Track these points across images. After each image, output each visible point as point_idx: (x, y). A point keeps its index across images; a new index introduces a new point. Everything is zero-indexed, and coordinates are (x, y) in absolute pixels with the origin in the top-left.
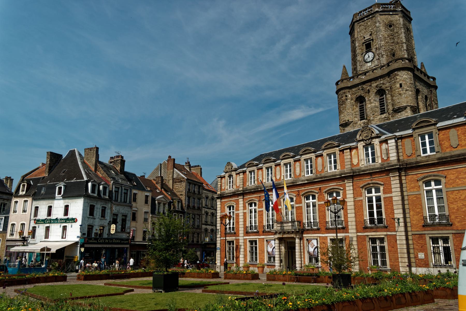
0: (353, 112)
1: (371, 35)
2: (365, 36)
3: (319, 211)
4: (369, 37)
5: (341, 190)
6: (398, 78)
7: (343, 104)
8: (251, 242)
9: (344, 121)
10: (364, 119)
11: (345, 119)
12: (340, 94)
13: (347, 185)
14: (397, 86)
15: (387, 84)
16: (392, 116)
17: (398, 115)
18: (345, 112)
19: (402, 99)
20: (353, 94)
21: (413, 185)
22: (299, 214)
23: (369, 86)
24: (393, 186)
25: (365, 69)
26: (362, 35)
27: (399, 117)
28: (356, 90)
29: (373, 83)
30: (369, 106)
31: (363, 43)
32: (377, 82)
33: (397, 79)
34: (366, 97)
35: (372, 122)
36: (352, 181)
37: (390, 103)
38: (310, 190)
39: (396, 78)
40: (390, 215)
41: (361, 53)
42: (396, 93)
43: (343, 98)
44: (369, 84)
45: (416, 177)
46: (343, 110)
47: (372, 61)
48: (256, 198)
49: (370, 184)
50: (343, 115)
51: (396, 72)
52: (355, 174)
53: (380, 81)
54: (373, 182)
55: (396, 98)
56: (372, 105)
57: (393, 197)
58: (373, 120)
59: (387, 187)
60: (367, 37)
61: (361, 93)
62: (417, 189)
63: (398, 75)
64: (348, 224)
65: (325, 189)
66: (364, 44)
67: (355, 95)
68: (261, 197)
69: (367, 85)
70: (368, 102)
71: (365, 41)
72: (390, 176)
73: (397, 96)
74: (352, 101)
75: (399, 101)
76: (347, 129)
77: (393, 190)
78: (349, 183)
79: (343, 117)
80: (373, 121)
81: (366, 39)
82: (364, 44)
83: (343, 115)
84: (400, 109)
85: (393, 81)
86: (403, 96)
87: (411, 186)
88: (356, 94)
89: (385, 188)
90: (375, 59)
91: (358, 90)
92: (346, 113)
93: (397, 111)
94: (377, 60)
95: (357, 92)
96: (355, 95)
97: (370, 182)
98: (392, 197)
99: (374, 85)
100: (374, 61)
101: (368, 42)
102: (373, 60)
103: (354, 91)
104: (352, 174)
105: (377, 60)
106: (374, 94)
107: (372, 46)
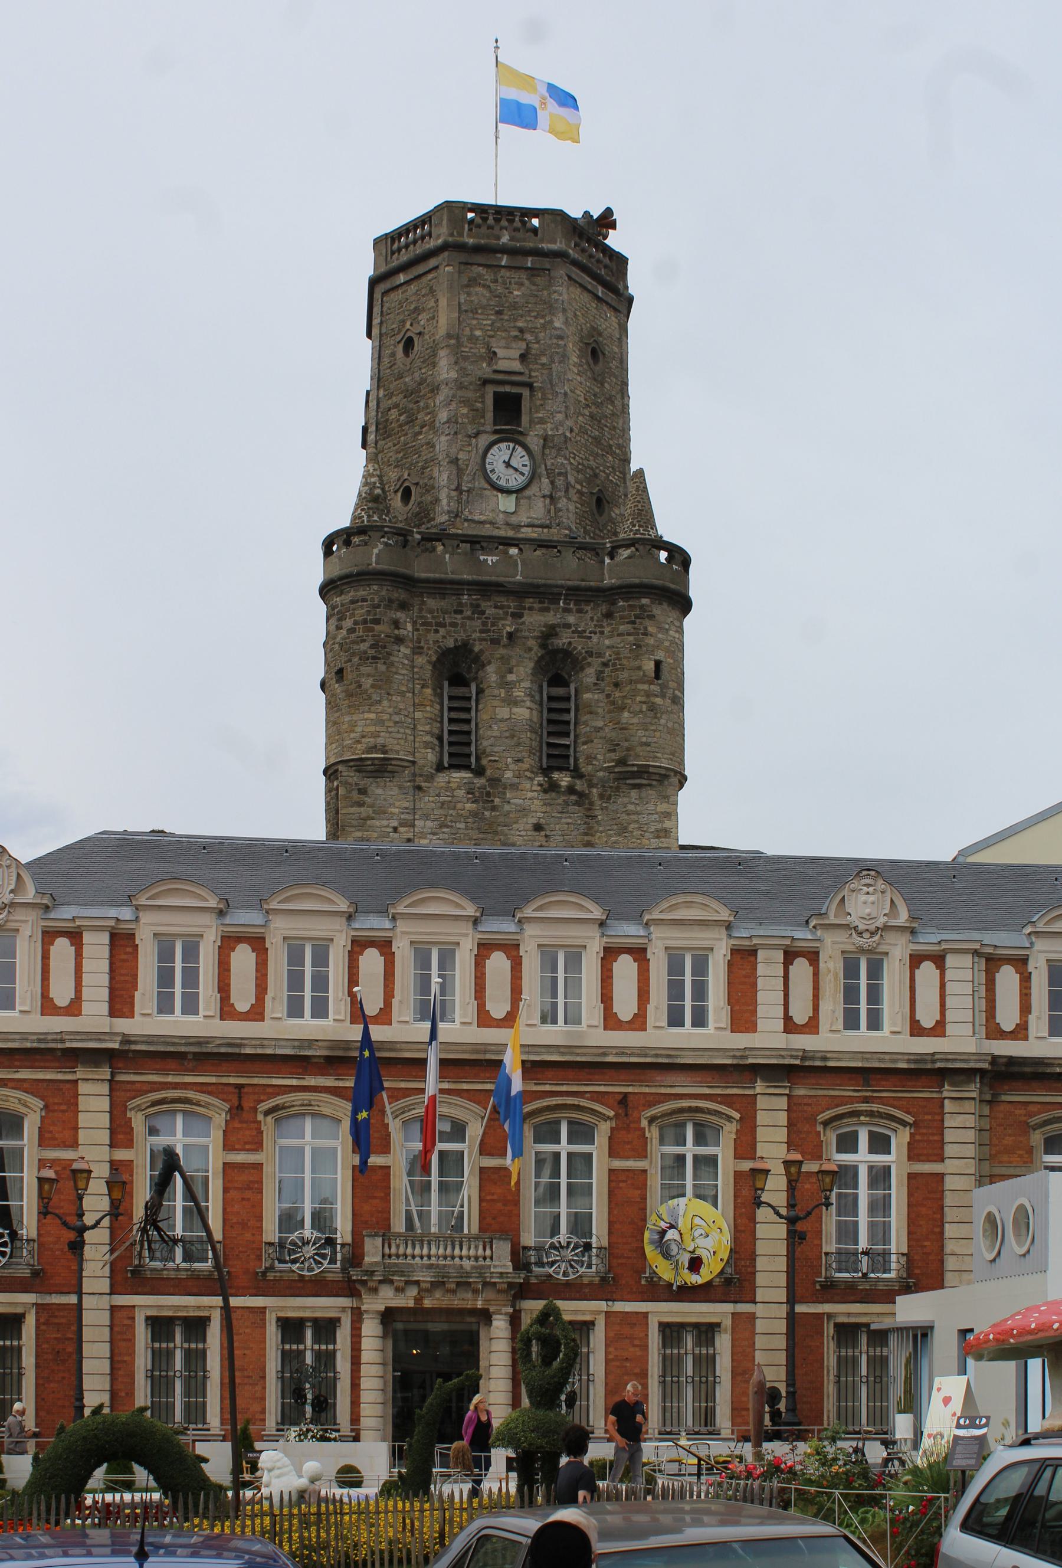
0: (418, 715)
1: (523, 357)
2: (501, 353)
3: (610, 1202)
4: (517, 366)
5: (729, 1118)
6: (650, 629)
7: (374, 658)
8: (291, 1328)
9: (373, 749)
10: (467, 767)
11: (380, 741)
12: (364, 600)
13: (761, 1103)
14: (645, 668)
15: (595, 638)
16: (601, 796)
17: (626, 800)
18: (385, 703)
19: (658, 734)
20: (423, 624)
21: (1008, 1141)
22: (499, 1205)
23: (513, 615)
24: (949, 1136)
25: (483, 518)
26: (478, 333)
27: (631, 807)
28: (445, 612)
29: (531, 609)
30: (503, 712)
31: (486, 382)
32: (547, 610)
33: (645, 634)
34: (489, 663)
35: (508, 795)
36: (787, 1091)
37: (598, 729)
38: (570, 1101)
39: (646, 628)
40: (926, 1243)
41: (471, 430)
42: (639, 699)
43: (377, 627)
44: (512, 604)
45: (1023, 1112)
46: (373, 686)
47: (518, 491)
48: (209, 1093)
49: (859, 1116)
50: (372, 716)
51: (645, 601)
52: (807, 1064)
53: (566, 610)
54: (875, 1107)
55: (635, 720)
56: (515, 710)
57: (947, 1179)
58: (514, 787)
59: (923, 1134)
60: (508, 359)
61: (472, 631)
62: (1021, 1156)
63: (652, 617)
64: (754, 1267)
65: (651, 1104)
66: (490, 390)
67: (437, 631)
68: (246, 1090)
69: (501, 607)
70: (496, 692)
71: (496, 372)
72: (945, 1094)
73: (641, 711)
74: (420, 660)
75: (644, 740)
76: (379, 791)
77: (949, 1150)
78: (773, 1097)
79: (372, 729)
80: (514, 794)
81: (502, 365)
82: (490, 390)
83: (372, 716)
84: (646, 776)
85: (631, 638)
86: (663, 721)
87: (1005, 1142)
88: (442, 631)
89: (918, 1137)
90: (533, 490)
91: (456, 612)
92: (391, 710)
93: (628, 782)
94: (544, 497)
95: (448, 621)
96: (437, 631)
97: (864, 1107)
98: (940, 1177)
99: (535, 620)
100: (529, 498)
101: (508, 389)
102: (527, 493)
103: (431, 611)
104: (798, 1062)
105: (544, 497)
106: (532, 665)
107: (525, 419)
